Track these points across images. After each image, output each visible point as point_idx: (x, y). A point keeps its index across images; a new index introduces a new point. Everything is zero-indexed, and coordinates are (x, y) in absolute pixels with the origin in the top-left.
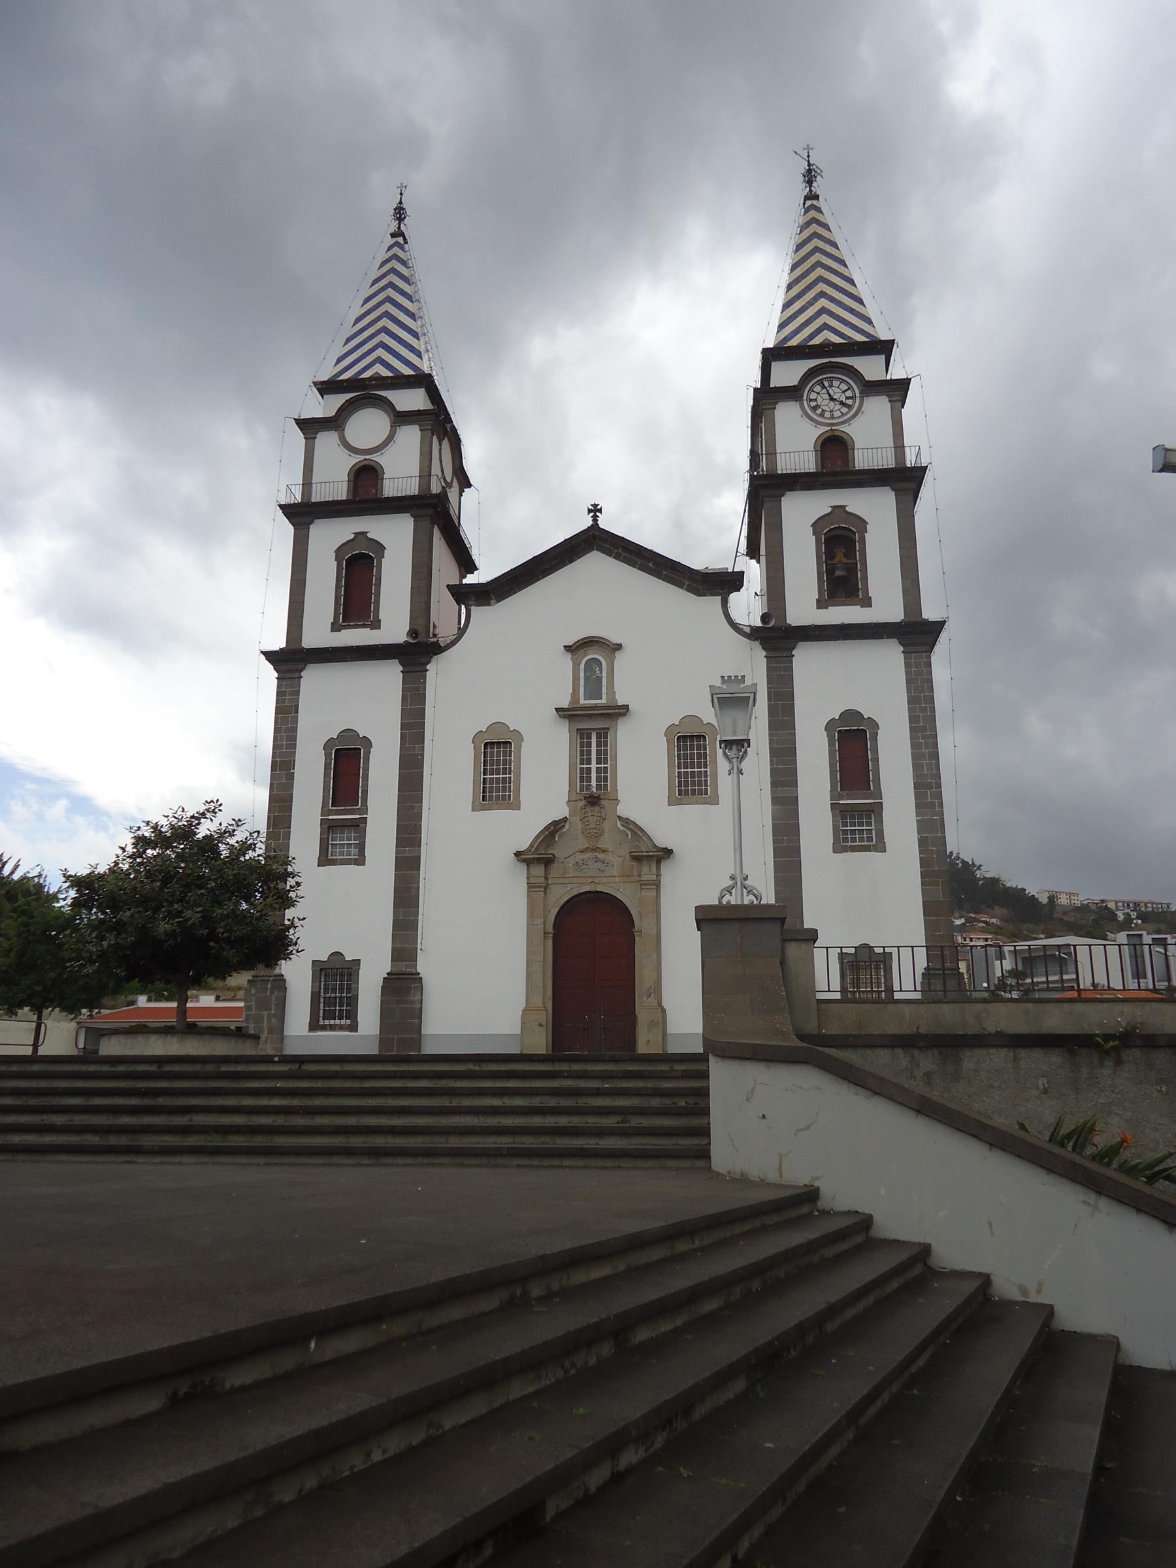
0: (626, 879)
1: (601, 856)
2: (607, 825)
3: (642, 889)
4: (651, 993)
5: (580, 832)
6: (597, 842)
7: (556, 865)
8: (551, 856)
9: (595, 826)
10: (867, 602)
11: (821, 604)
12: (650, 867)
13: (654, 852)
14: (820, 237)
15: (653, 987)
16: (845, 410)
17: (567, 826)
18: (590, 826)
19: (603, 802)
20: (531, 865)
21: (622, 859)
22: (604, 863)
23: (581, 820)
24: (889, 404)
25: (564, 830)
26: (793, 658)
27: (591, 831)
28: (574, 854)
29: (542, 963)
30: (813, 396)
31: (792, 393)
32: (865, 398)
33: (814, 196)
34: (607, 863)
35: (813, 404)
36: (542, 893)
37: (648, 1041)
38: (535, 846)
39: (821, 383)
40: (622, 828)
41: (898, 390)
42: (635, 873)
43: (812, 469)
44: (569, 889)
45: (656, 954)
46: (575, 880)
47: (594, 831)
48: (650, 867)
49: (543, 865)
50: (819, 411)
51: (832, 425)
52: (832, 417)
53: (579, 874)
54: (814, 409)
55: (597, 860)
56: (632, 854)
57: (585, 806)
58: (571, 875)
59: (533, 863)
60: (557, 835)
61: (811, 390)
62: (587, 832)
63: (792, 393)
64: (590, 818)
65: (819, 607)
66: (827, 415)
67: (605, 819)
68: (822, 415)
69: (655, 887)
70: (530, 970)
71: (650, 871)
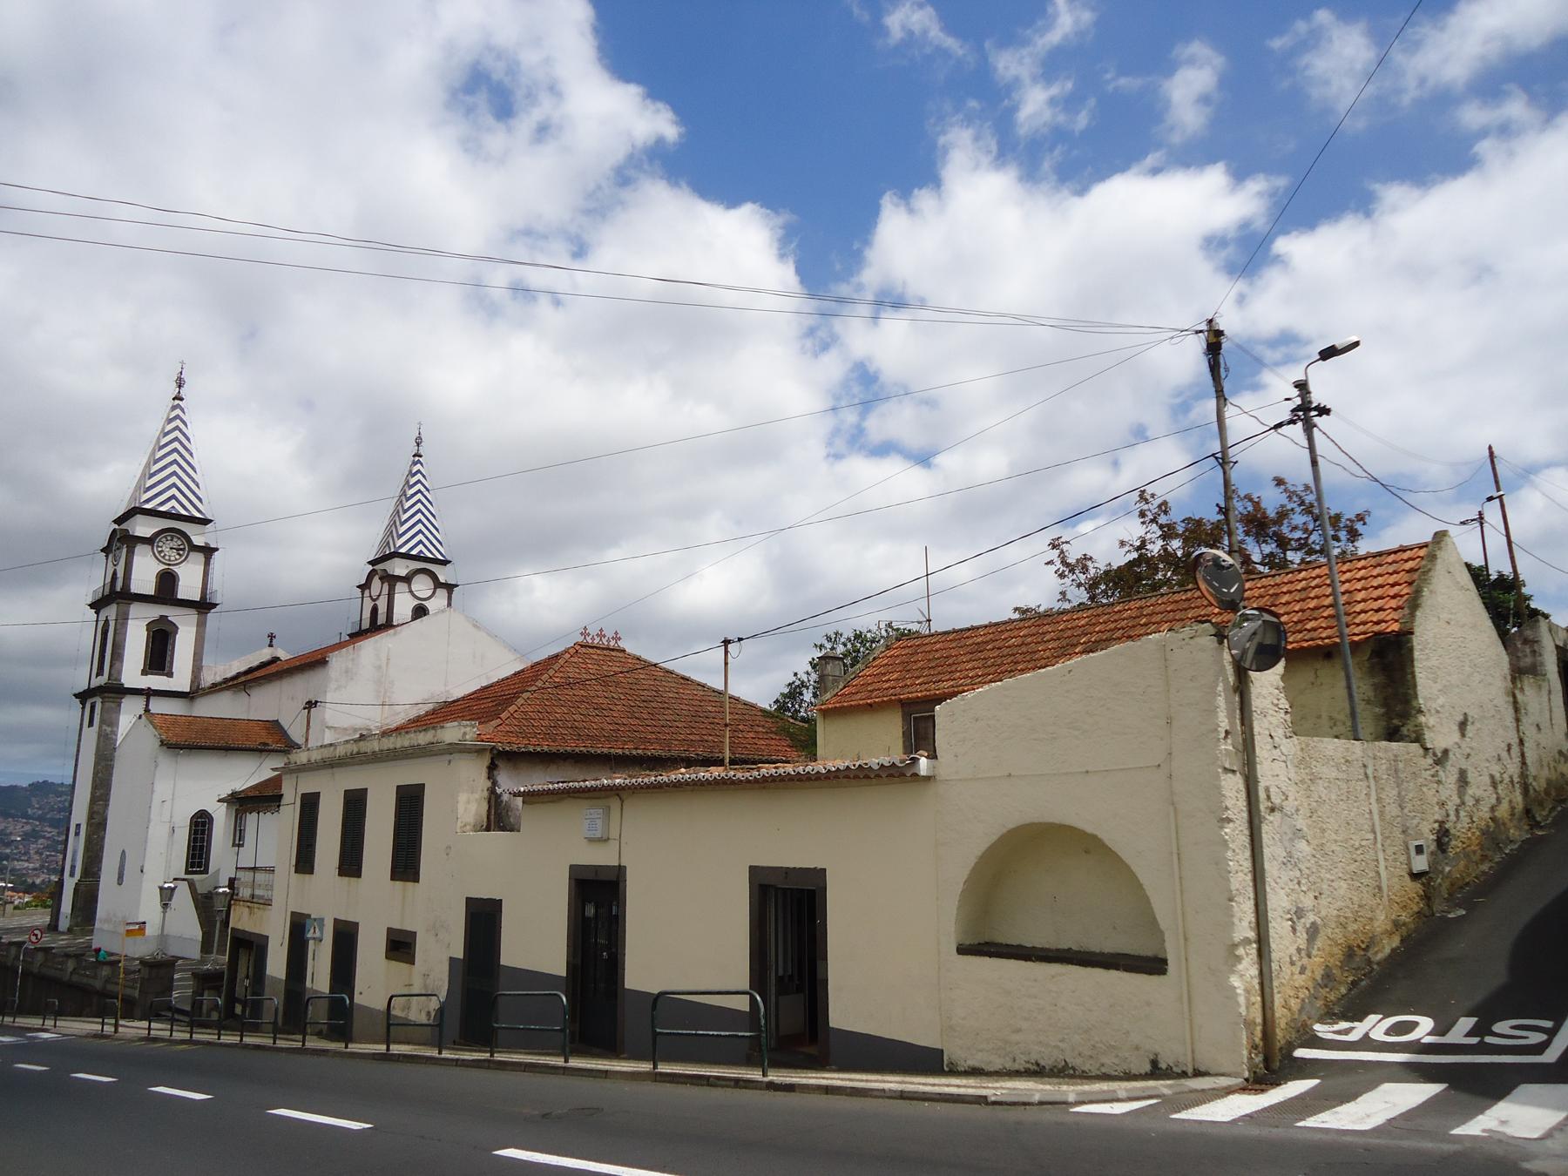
10: (170, 675)
11: (144, 673)
14: (181, 431)
16: (177, 557)
24: (204, 559)
26: (122, 705)
30: (161, 544)
31: (149, 541)
32: (191, 553)
33: (178, 398)
35: (160, 549)
39: (165, 537)
41: (208, 551)
43: (153, 594)
50: (162, 555)
51: (169, 565)
52: (170, 560)
54: (160, 552)
61: (160, 541)
63: (149, 541)
65: (142, 674)
66: (167, 558)
68: (163, 557)
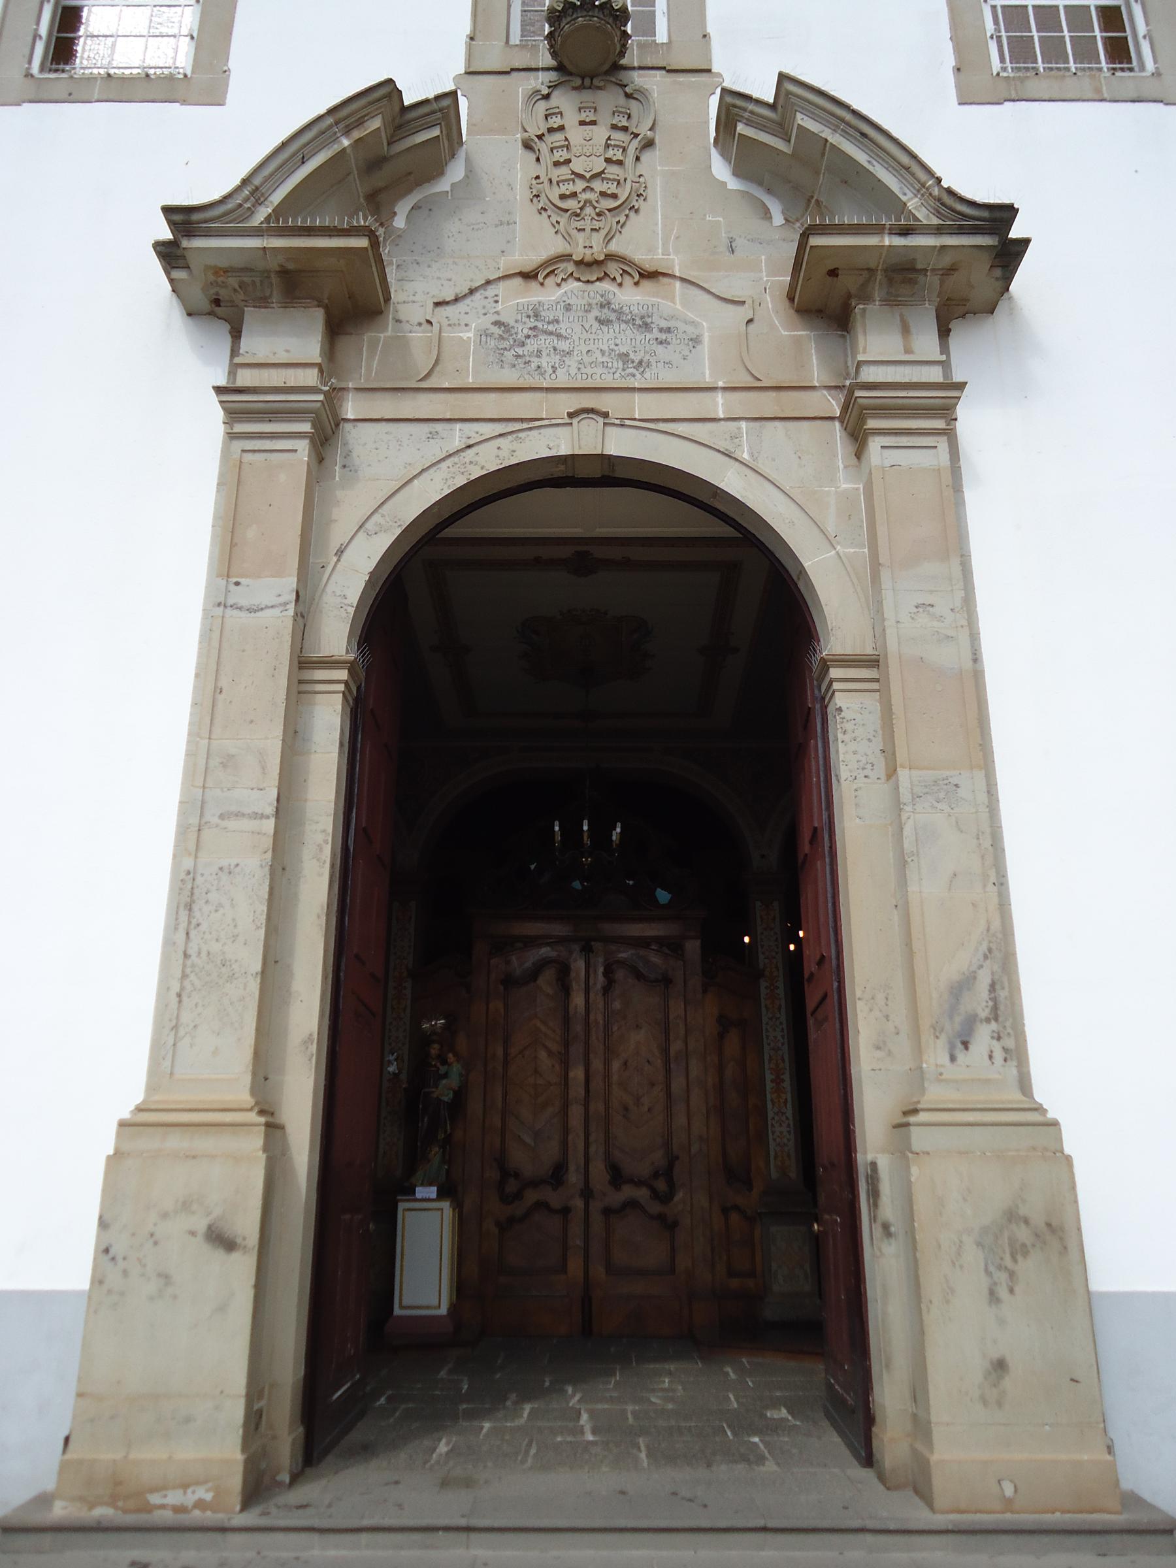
0: (767, 403)
1: (630, 296)
2: (654, 166)
3: (859, 453)
4: (970, 1023)
5: (521, 193)
6: (608, 239)
7: (389, 333)
8: (363, 243)
9: (599, 165)
12: (906, 330)
13: (939, 230)
15: (984, 979)
17: (456, 172)
18: (578, 166)
19: (638, 79)
20: (251, 315)
21: (744, 313)
22: (646, 326)
23: (527, 145)
25: (443, 185)
27: (580, 185)
28: (488, 282)
29: (269, 825)
34: (668, 330)
36: (303, 446)
37: (1000, 1365)
38: (277, 197)
40: (733, 184)
42: (816, 373)
44: (457, 444)
45: (980, 775)
46: (489, 405)
47: (598, 186)
48: (906, 330)
49: (319, 315)
53: (509, 377)
55: (609, 316)
56: (815, 241)
57: (553, 87)
58: (470, 381)
59: (263, 302)
60: (403, 209)
62: (566, 189)
64: (576, 135)
67: (649, 144)
69: (939, 424)
70: (188, 863)
71: (908, 351)
